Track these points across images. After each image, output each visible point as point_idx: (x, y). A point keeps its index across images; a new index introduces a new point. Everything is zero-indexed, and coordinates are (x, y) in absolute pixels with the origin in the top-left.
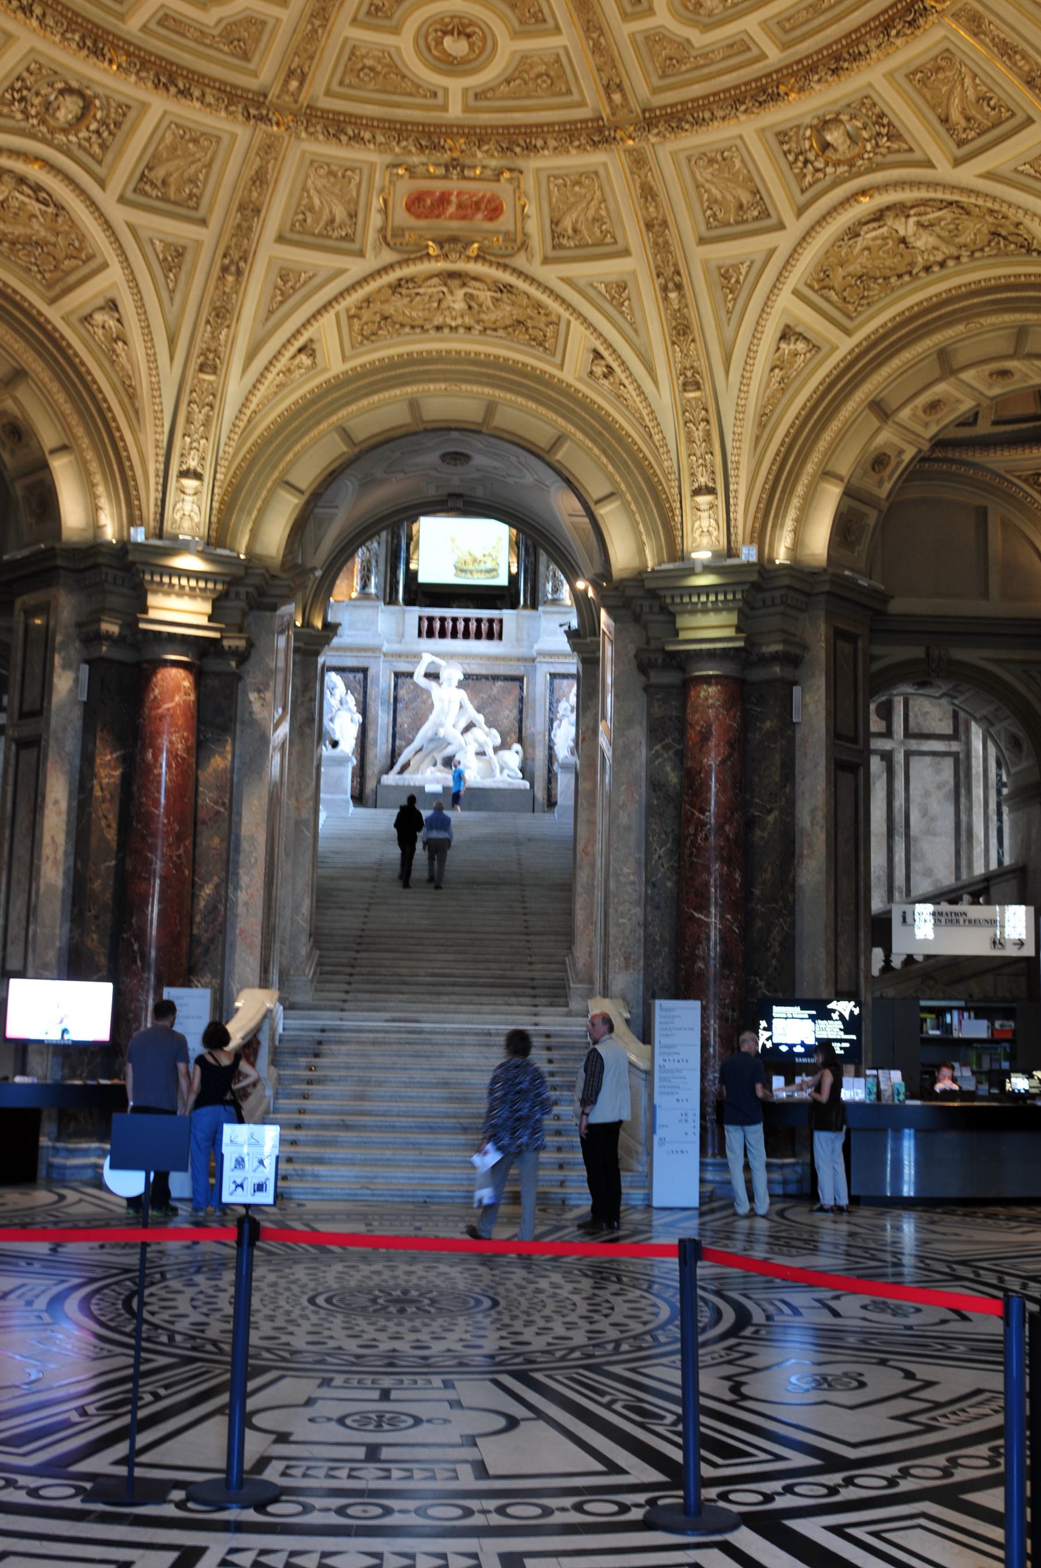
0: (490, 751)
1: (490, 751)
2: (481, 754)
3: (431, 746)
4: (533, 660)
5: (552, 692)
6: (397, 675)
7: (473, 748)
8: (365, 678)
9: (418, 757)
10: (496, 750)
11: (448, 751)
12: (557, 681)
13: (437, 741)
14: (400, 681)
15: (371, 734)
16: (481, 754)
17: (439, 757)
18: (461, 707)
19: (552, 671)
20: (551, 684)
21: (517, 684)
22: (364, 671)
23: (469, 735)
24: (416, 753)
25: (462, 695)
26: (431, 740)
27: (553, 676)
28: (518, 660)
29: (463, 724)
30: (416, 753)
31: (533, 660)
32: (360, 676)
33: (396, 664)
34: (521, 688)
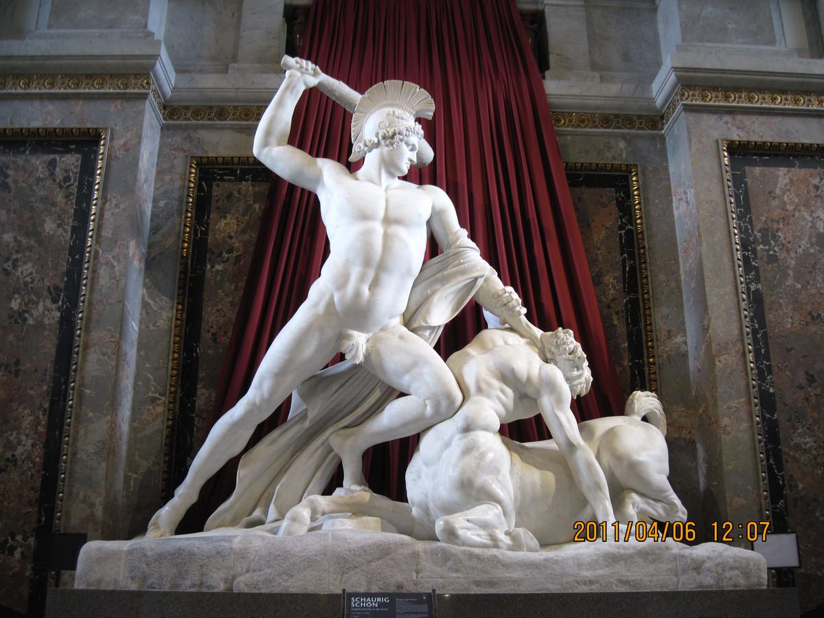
0: (564, 420)
1: (564, 420)
2: (523, 430)
3: (316, 410)
4: (655, 120)
5: (744, 204)
6: (210, 172)
7: (491, 409)
8: (88, 169)
9: (264, 449)
10: (584, 409)
11: (392, 418)
12: (755, 173)
13: (349, 385)
14: (216, 191)
15: (91, 364)
16: (523, 430)
17: (349, 450)
18: (434, 248)
19: (736, 135)
20: (738, 181)
21: (610, 192)
22: (85, 142)
23: (476, 361)
24: (262, 431)
25: (436, 198)
26: (315, 384)
27: (743, 153)
28: (606, 121)
29: (441, 313)
30: (262, 431)
31: (655, 120)
32: (71, 161)
33: (204, 135)
34: (625, 208)
